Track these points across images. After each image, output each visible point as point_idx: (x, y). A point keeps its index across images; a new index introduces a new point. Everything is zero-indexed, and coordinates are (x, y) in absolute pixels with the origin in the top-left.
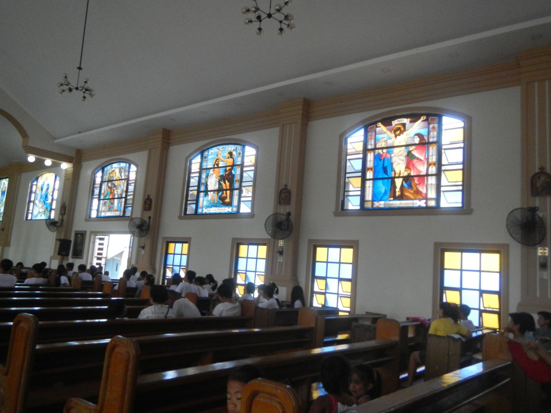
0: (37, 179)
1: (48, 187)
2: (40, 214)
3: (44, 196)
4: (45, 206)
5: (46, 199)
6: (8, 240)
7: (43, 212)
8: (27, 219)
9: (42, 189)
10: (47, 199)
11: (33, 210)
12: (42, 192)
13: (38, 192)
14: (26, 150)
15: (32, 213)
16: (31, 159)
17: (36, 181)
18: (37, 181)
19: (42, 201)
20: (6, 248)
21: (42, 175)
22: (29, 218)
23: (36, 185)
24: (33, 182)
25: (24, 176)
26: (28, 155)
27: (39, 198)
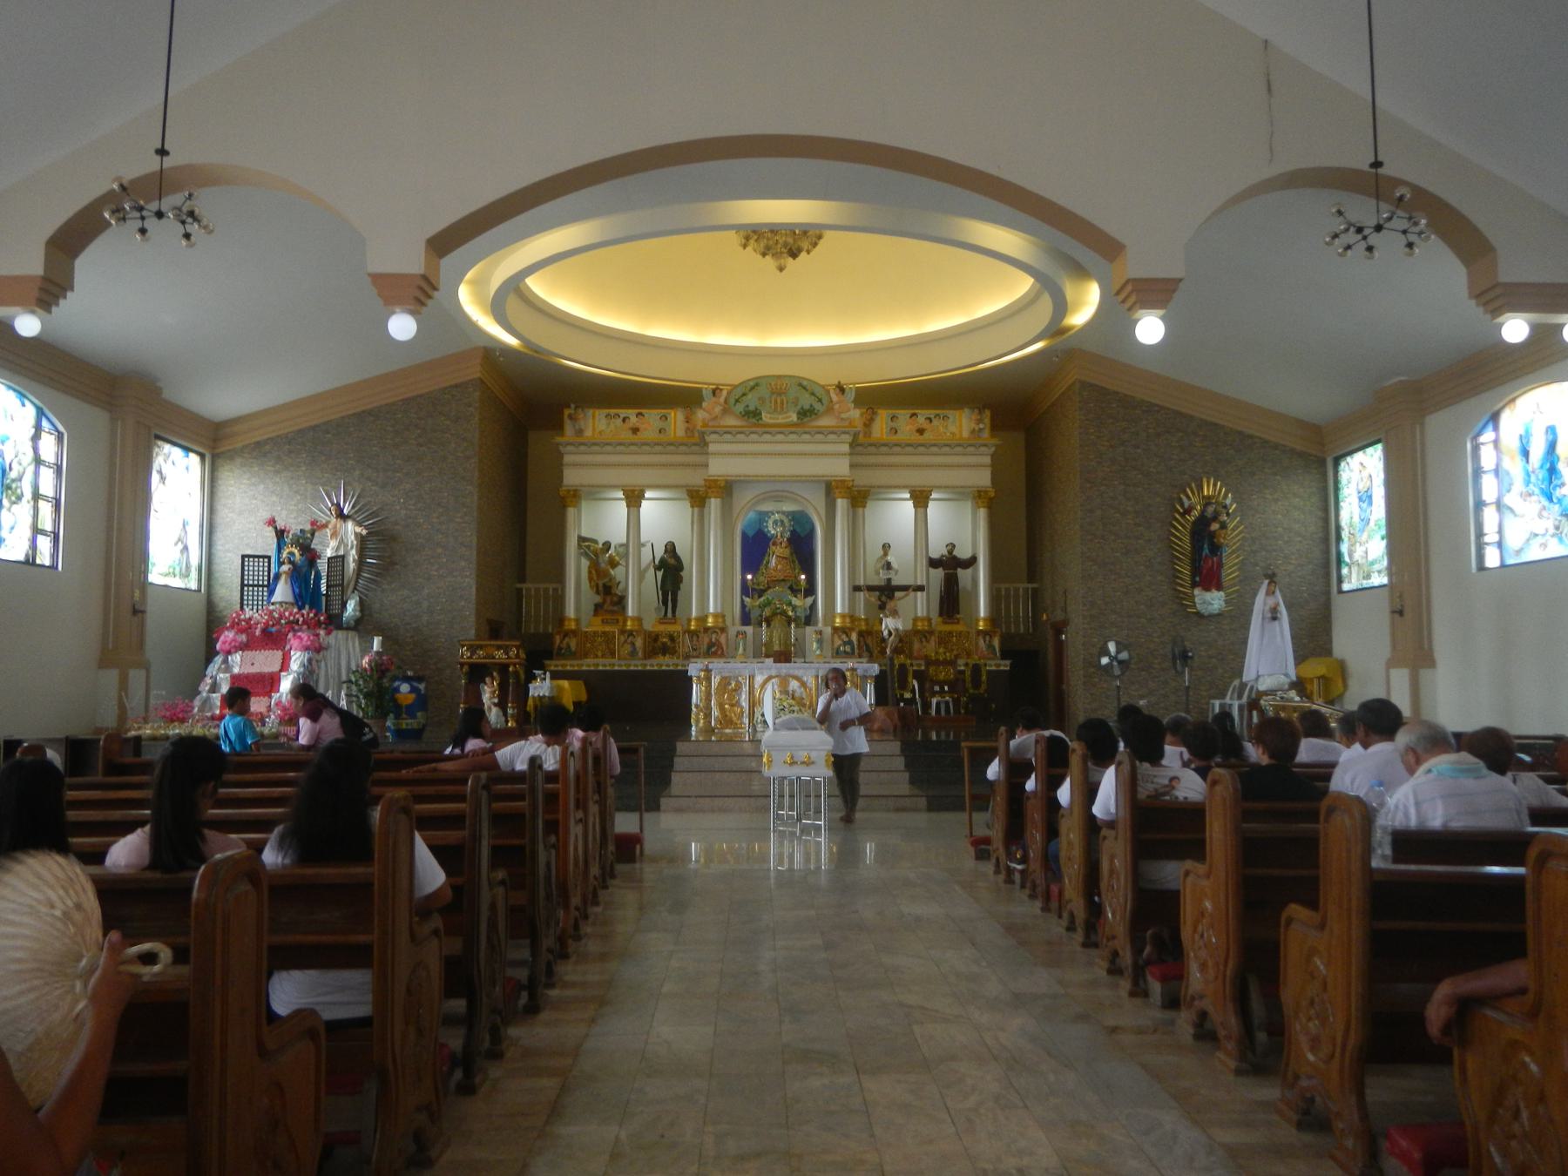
0: (1495, 418)
1: (1551, 437)
2: (1540, 540)
3: (1542, 474)
4: (1557, 507)
5: (1551, 482)
6: (1426, 646)
7: (1552, 531)
8: (1481, 567)
9: (1526, 454)
10: (1555, 482)
11: (1500, 531)
12: (1528, 462)
13: (1514, 466)
14: (1485, 304)
15: (1500, 545)
16: (1515, 329)
17: (1490, 427)
18: (1496, 429)
19: (1537, 491)
20: (1425, 674)
21: (1513, 400)
22: (1492, 559)
23: (1496, 442)
24: (1479, 434)
25: (1437, 423)
26: (1500, 320)
27: (1519, 485)
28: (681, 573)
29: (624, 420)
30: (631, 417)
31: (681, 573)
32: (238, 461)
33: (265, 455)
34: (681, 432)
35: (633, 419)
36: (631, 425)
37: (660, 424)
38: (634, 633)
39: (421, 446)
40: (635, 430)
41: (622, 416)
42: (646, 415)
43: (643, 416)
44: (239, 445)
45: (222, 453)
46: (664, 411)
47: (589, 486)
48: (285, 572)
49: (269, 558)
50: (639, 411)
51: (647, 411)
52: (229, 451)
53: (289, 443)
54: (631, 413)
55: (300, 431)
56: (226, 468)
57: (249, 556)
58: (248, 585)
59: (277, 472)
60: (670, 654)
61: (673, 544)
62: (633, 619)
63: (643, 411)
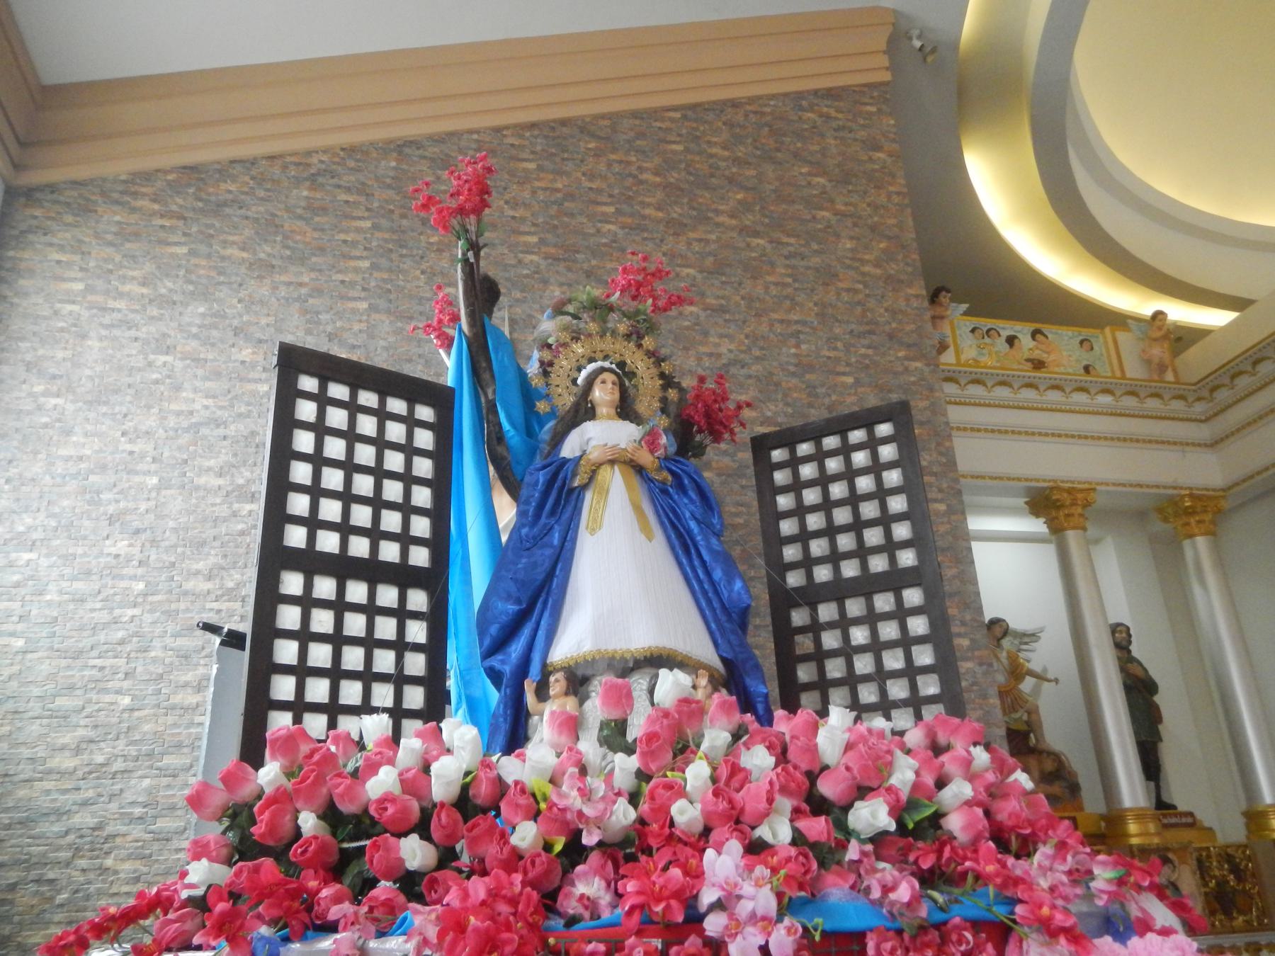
28: (1157, 699)
29: (1011, 340)
30: (1018, 335)
31: (1157, 699)
32: (112, 217)
33: (218, 208)
34: (1135, 370)
35: (1026, 342)
36: (1027, 355)
37: (1086, 358)
38: (1171, 855)
39: (756, 234)
40: (1038, 365)
41: (1005, 334)
42: (1050, 336)
43: (1047, 337)
44: (122, 168)
45: (52, 188)
46: (1086, 332)
47: (972, 477)
48: (618, 460)
49: (441, 398)
50: (1038, 326)
51: (1054, 328)
52: (76, 184)
53: (314, 186)
54: (1022, 330)
55: (351, 150)
56: (64, 236)
57: (328, 368)
58: (311, 563)
59: (264, 268)
60: (1241, 912)
61: (1128, 629)
62: (1140, 815)
63: (1046, 328)
